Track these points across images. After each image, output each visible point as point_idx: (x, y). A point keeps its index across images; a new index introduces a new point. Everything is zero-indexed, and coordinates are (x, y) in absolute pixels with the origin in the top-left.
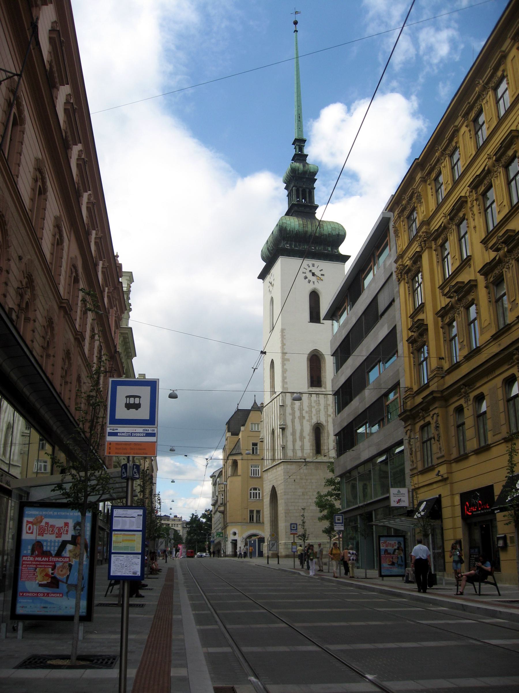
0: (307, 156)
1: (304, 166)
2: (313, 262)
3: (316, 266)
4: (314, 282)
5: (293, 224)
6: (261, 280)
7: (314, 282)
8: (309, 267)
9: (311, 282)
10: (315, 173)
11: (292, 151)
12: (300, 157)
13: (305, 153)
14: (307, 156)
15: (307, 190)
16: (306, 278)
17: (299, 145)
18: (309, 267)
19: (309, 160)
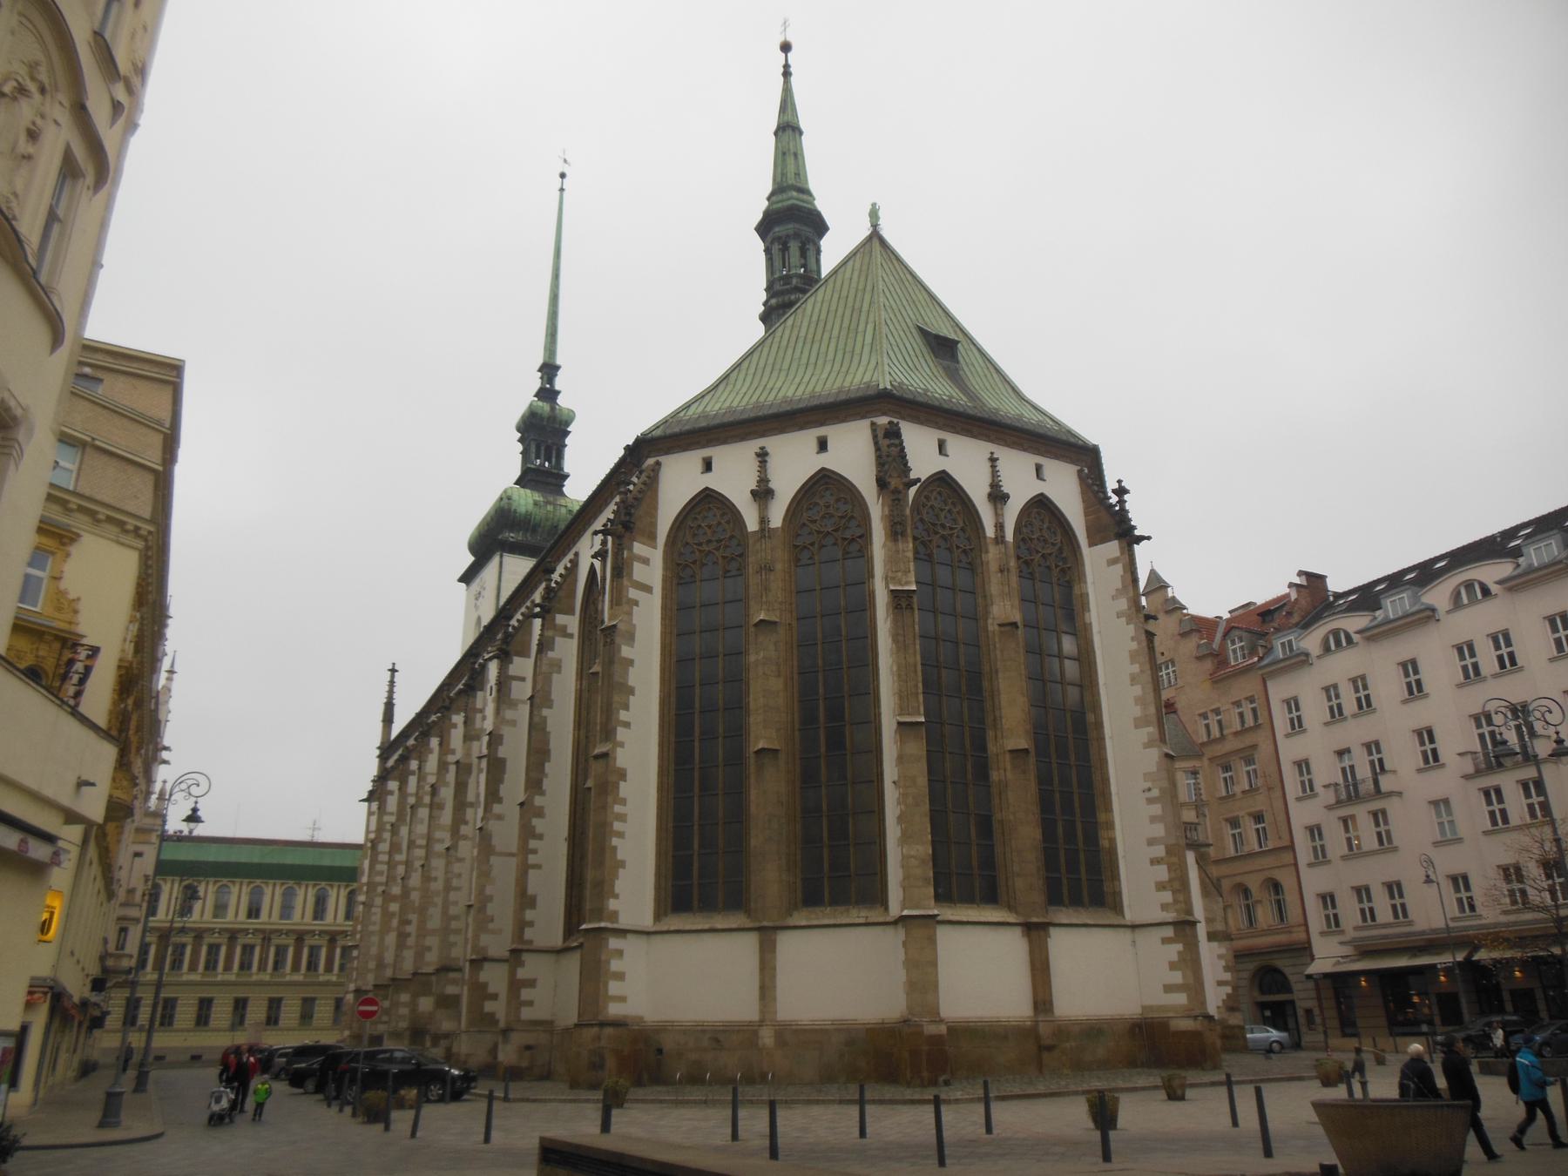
0: (558, 393)
5: (522, 502)
10: (568, 423)
11: (536, 383)
12: (548, 393)
13: (557, 387)
14: (558, 393)
19: (561, 400)
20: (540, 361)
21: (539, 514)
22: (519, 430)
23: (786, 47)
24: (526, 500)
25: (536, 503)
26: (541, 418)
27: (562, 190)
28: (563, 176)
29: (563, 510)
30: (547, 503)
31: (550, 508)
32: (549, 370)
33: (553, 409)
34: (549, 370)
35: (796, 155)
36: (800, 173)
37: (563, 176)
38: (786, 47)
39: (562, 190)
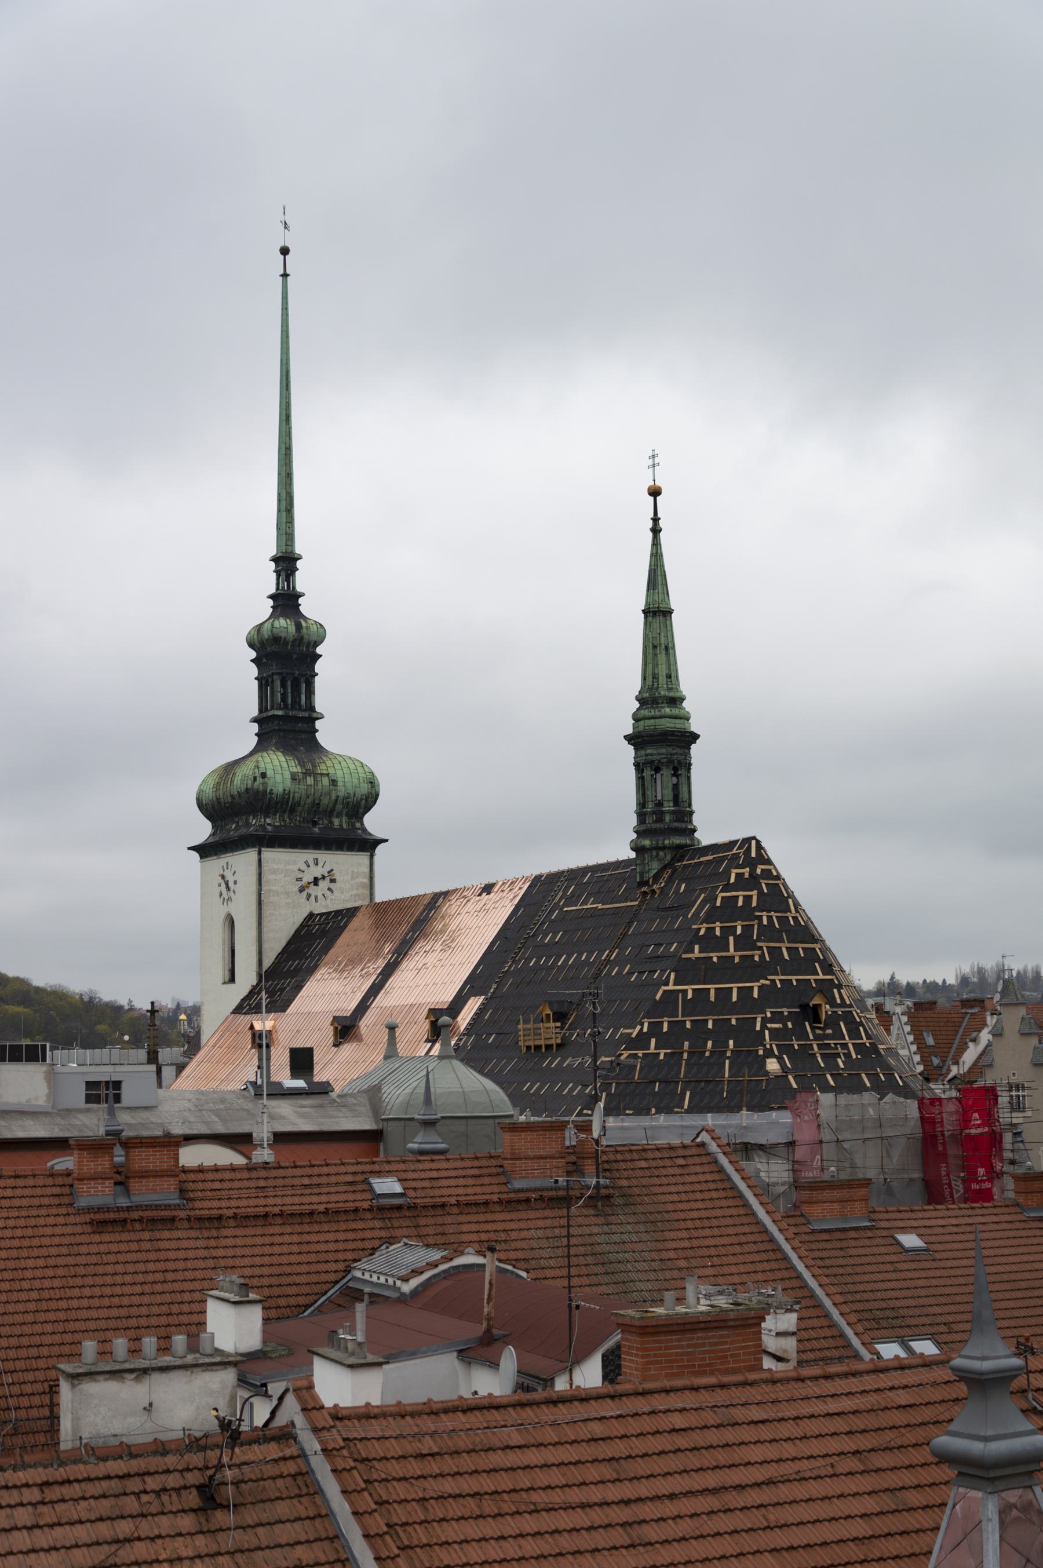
1: (299, 627)
2: (316, 856)
3: (321, 863)
4: (316, 897)
5: (279, 778)
6: (195, 855)
7: (316, 897)
8: (309, 866)
9: (312, 898)
11: (269, 583)
13: (299, 588)
15: (303, 679)
16: (302, 890)
17: (286, 571)
18: (309, 866)
19: (306, 606)
20: (273, 552)
21: (299, 790)
22: (251, 645)
23: (655, 493)
24: (279, 769)
25: (294, 777)
26: (286, 642)
27: (285, 275)
28: (285, 251)
29: (326, 781)
30: (306, 774)
31: (310, 780)
32: (286, 563)
33: (299, 627)
34: (286, 563)
35: (667, 648)
36: (671, 676)
37: (285, 251)
38: (655, 493)
39: (285, 275)
